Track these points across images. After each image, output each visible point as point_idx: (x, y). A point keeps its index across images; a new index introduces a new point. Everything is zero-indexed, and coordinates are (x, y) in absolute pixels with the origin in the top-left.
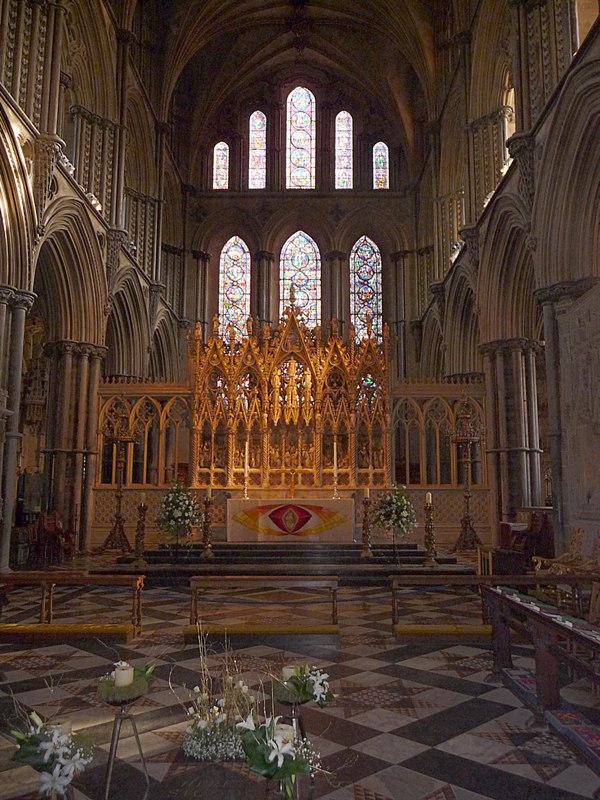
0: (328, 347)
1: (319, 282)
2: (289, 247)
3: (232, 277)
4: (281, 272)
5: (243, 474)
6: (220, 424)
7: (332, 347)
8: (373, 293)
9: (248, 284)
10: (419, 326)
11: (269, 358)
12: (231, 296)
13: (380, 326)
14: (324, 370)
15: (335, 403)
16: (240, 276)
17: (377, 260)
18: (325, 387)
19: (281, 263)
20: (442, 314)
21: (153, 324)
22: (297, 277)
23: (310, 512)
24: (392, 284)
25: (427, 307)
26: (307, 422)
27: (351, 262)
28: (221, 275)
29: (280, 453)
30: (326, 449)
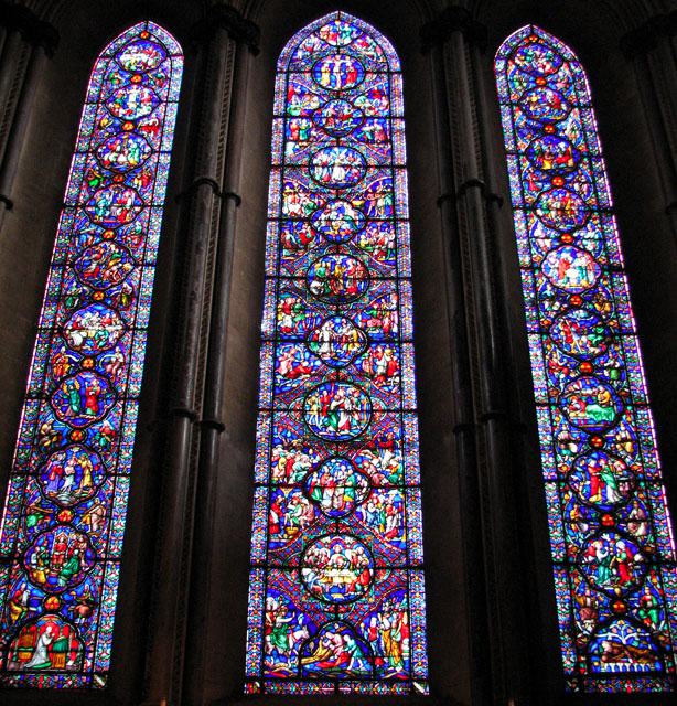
1: (400, 125)
8: (578, 156)
9: (170, 129)
12: (110, 157)
13: (615, 245)
16: (145, 110)
19: (280, 82)
22: (329, 111)
28: (87, 108)
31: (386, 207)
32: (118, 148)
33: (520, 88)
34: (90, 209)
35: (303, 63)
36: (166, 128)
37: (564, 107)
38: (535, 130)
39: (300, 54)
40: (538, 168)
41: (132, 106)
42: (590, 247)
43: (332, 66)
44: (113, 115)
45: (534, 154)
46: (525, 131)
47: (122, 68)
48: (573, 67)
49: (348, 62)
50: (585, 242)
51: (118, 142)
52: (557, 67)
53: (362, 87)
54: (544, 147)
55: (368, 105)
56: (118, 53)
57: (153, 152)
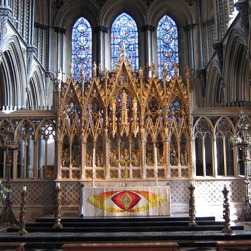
0: (148, 83)
1: (137, 46)
2: (117, 23)
3: (80, 44)
4: (112, 40)
5: (92, 171)
6: (76, 136)
7: (151, 83)
8: (173, 52)
9: (91, 48)
10: (204, 72)
11: (107, 91)
12: (79, 56)
14: (146, 99)
15: (154, 121)
16: (85, 43)
17: (175, 30)
18: (146, 110)
19: (112, 34)
20: (221, 63)
21: (28, 71)
23: (140, 195)
24: (185, 45)
25: (209, 61)
26: (136, 134)
27: (158, 32)
28: (73, 43)
29: (117, 156)
30: (150, 152)
31: (134, 67)
32: (81, 54)
33: (162, 34)
34: (77, 69)
35: (117, 29)
36: (90, 48)
37: (171, 39)
38: (165, 46)
39: (116, 27)
40: (165, 56)
41: (82, 42)
42: (173, 75)
43: (123, 30)
44: (79, 45)
45: (164, 52)
46: (163, 46)
47: (79, 31)
48: (174, 28)
49: (126, 29)
50: (172, 74)
51: (81, 52)
52: (171, 28)
53: (129, 36)
54: (166, 51)
55: (130, 41)
56: (77, 27)
57: (88, 54)
